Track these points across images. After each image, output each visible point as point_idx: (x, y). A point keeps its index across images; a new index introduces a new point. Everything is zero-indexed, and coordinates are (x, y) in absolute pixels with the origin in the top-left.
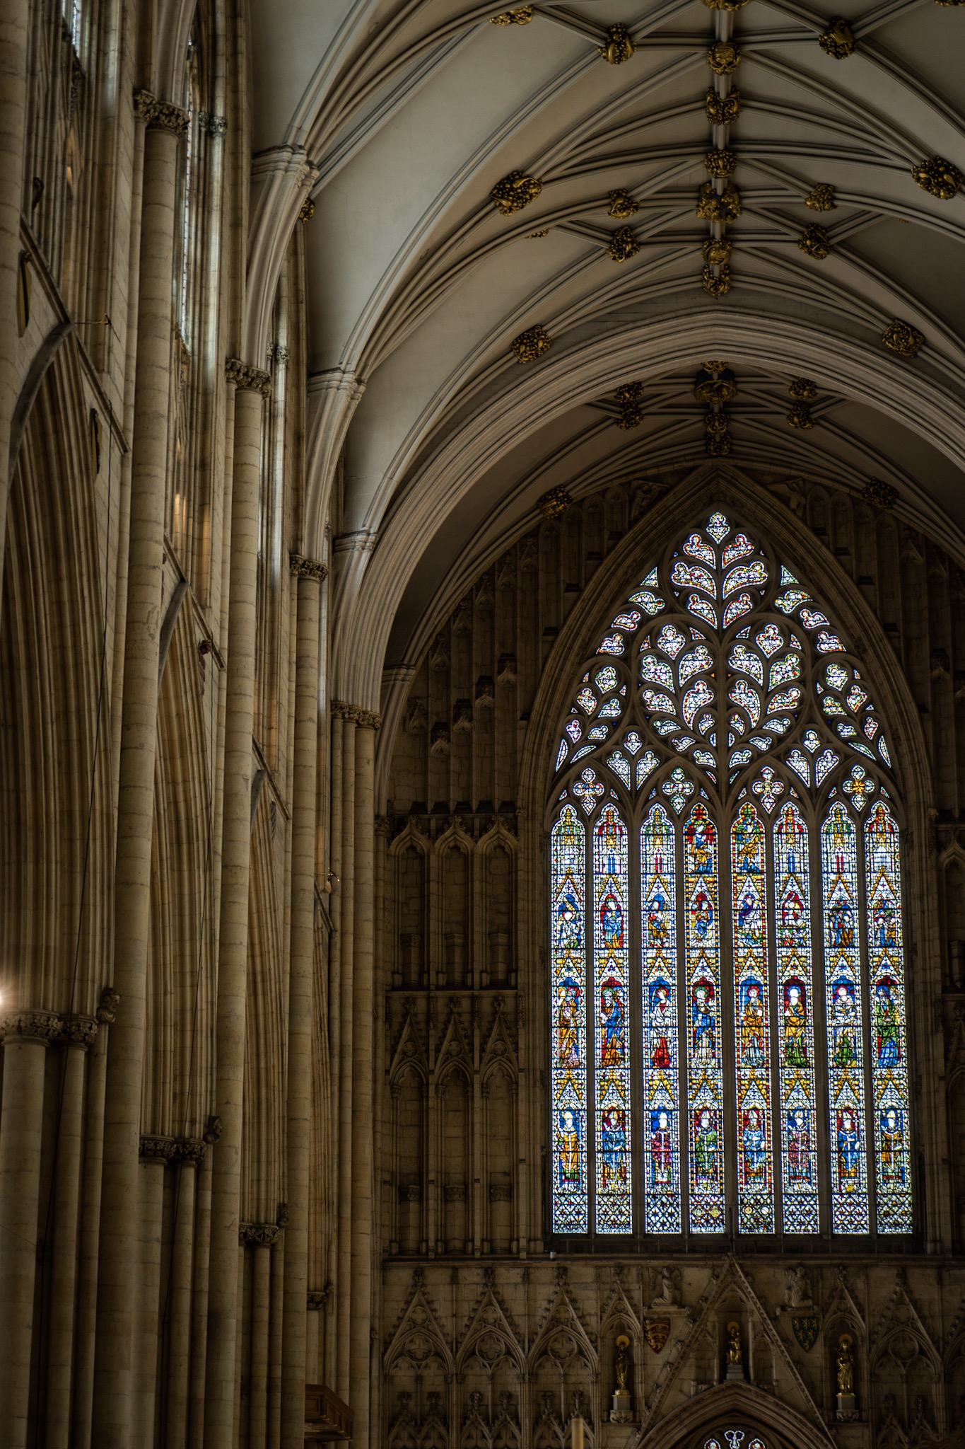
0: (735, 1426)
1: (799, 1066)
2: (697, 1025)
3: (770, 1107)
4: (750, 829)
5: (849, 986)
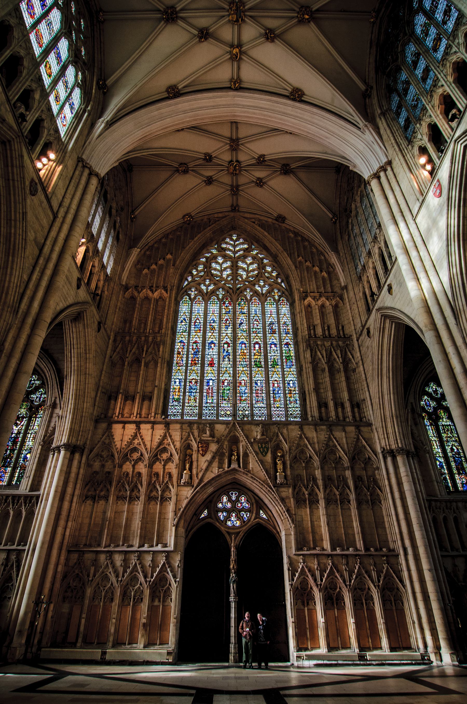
0: (234, 489)
5: (275, 345)
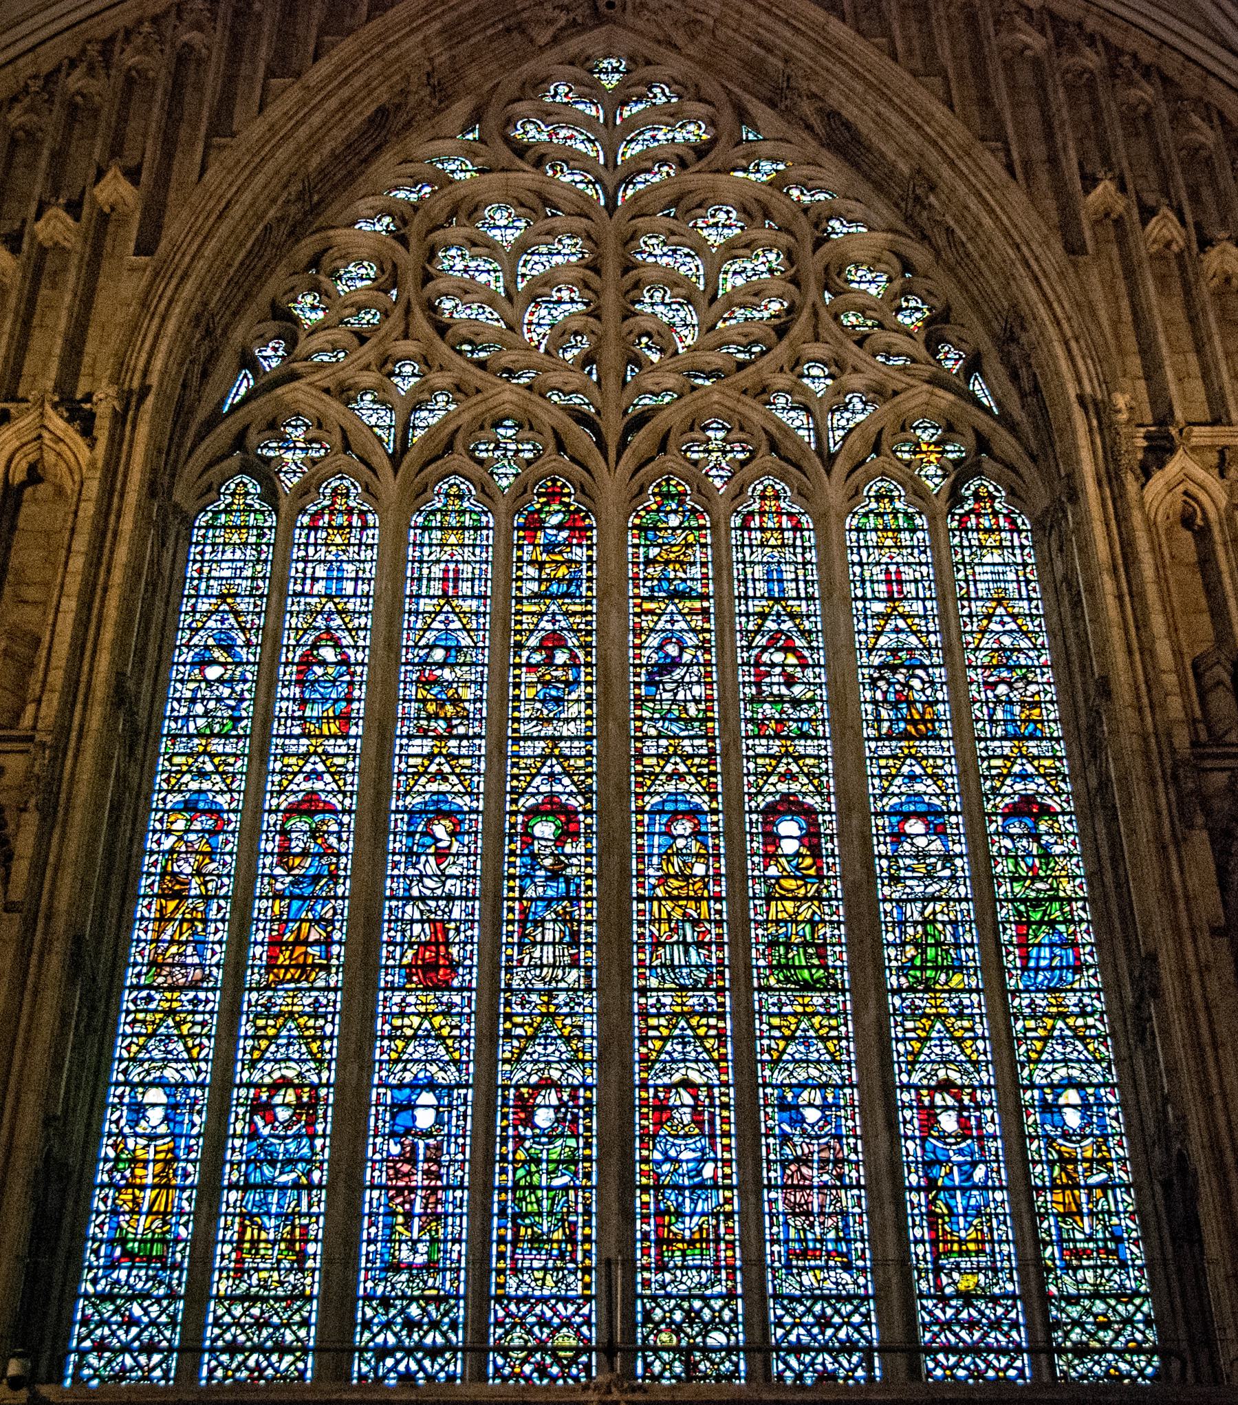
1: (807, 987)
2: (530, 893)
3: (730, 1078)
4: (674, 521)
